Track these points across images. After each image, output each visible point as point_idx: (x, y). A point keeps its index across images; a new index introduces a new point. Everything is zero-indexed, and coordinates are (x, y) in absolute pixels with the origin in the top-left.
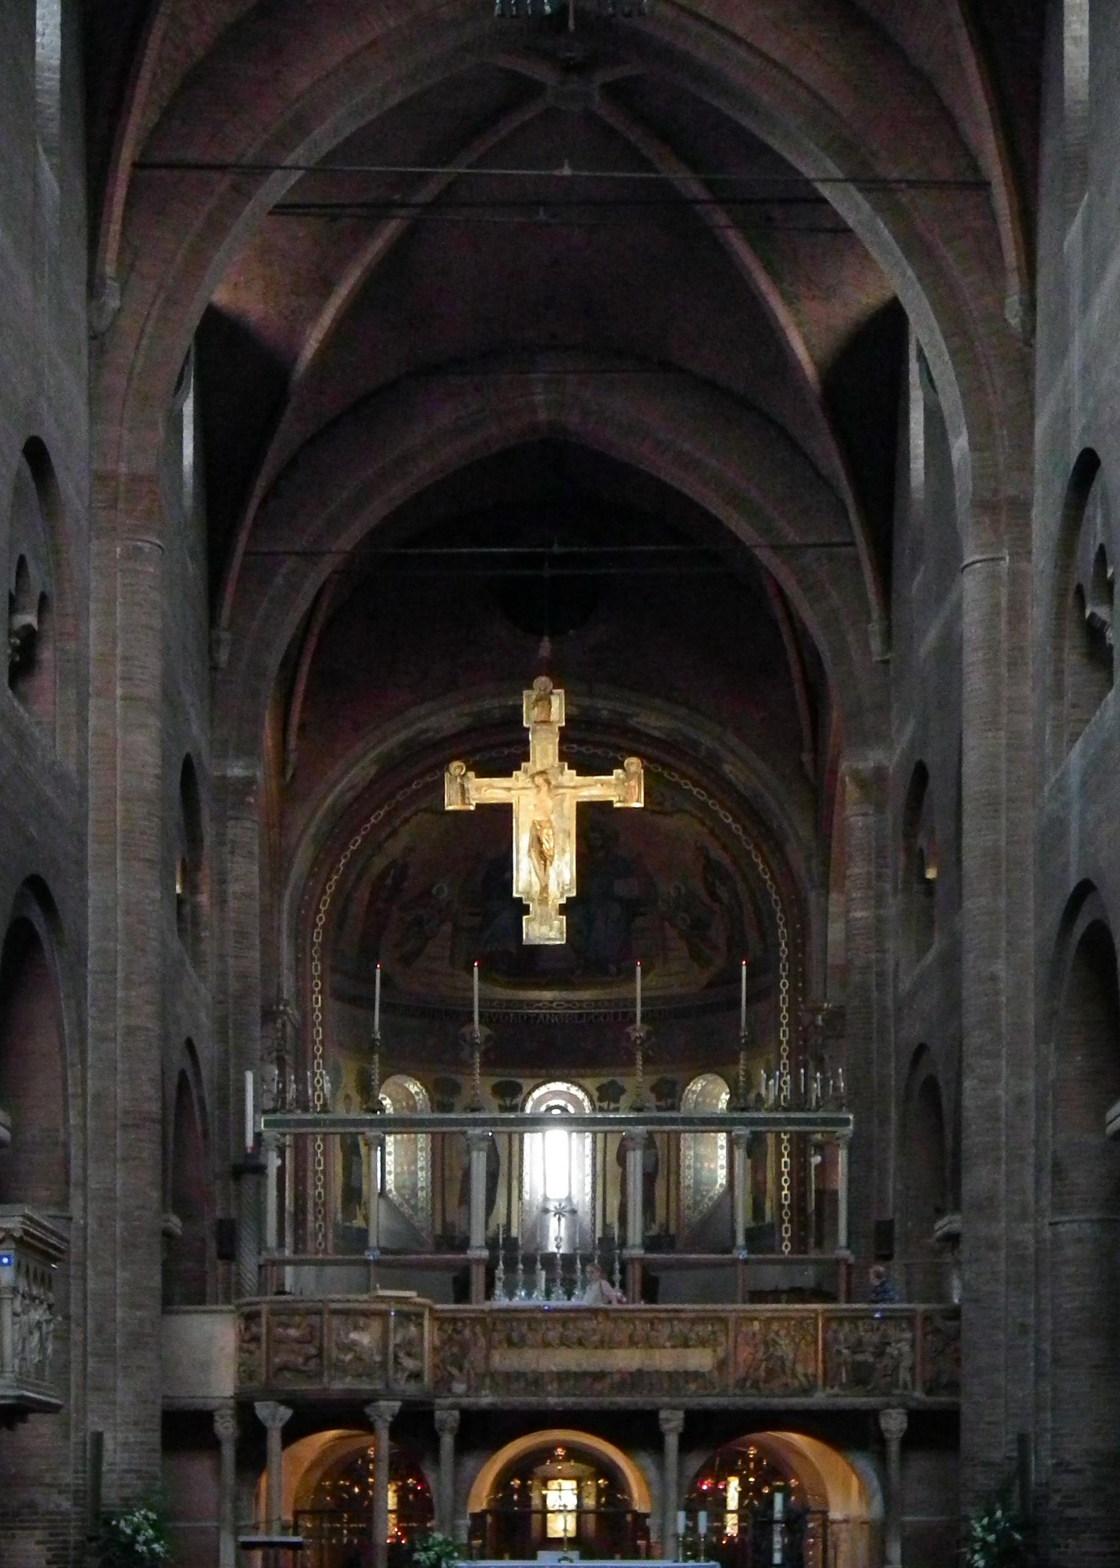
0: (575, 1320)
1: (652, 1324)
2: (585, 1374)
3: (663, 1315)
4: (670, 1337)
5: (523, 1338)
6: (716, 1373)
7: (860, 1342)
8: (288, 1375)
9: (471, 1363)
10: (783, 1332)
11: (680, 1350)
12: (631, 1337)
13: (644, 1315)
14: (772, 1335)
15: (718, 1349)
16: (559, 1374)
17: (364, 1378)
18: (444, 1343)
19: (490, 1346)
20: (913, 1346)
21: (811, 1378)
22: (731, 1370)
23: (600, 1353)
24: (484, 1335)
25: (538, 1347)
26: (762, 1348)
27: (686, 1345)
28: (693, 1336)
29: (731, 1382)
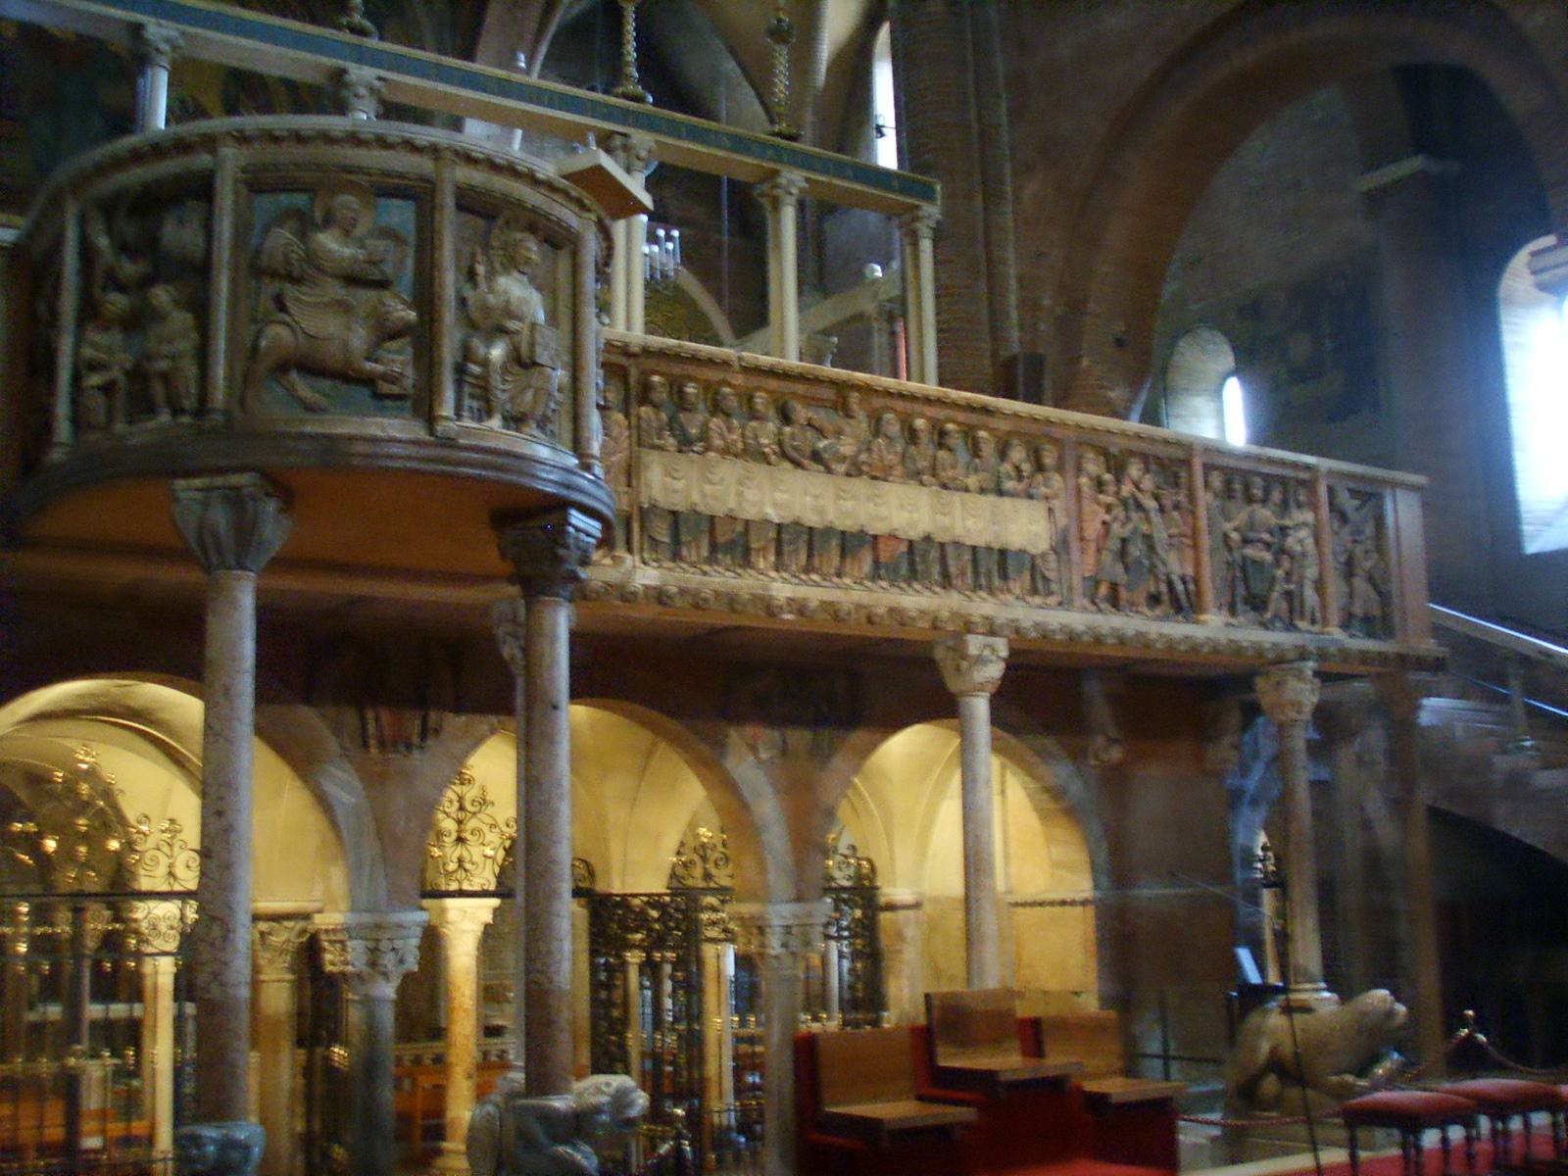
2: (828, 531)
6: (1052, 557)
7: (1252, 525)
8: (303, 387)
10: (1148, 483)
14: (1127, 489)
16: (780, 527)
17: (532, 428)
20: (1317, 541)
21: (1191, 587)
22: (1075, 556)
23: (860, 485)
25: (736, 456)
26: (1122, 515)
27: (1000, 492)
29: (1076, 581)
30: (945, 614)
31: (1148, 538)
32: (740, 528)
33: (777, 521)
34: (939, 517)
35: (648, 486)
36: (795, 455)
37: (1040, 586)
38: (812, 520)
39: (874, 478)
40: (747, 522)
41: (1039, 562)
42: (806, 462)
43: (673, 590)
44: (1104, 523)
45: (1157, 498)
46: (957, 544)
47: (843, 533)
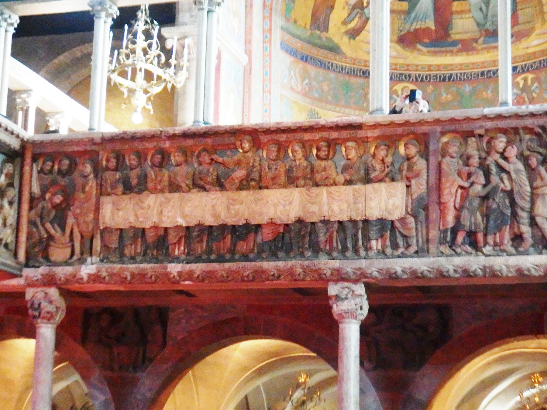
0: (214, 150)
1: (318, 149)
2: (223, 227)
3: (334, 135)
4: (345, 169)
5: (143, 178)
6: (411, 220)
9: (76, 217)
10: (512, 152)
11: (359, 187)
12: (289, 171)
13: (307, 136)
15: (413, 181)
16: (188, 228)
18: (44, 190)
19: (102, 192)
22: (434, 214)
24: (96, 177)
25: (162, 191)
27: (367, 180)
28: (378, 166)
29: (434, 234)
30: (299, 270)
31: (510, 194)
32: (162, 233)
33: (184, 225)
34: (309, 205)
35: (104, 217)
36: (202, 183)
37: (400, 241)
38: (209, 221)
39: (260, 188)
40: (166, 229)
41: (397, 224)
42: (207, 187)
43: (104, 274)
44: (461, 187)
45: (525, 159)
46: (326, 222)
47: (234, 226)
